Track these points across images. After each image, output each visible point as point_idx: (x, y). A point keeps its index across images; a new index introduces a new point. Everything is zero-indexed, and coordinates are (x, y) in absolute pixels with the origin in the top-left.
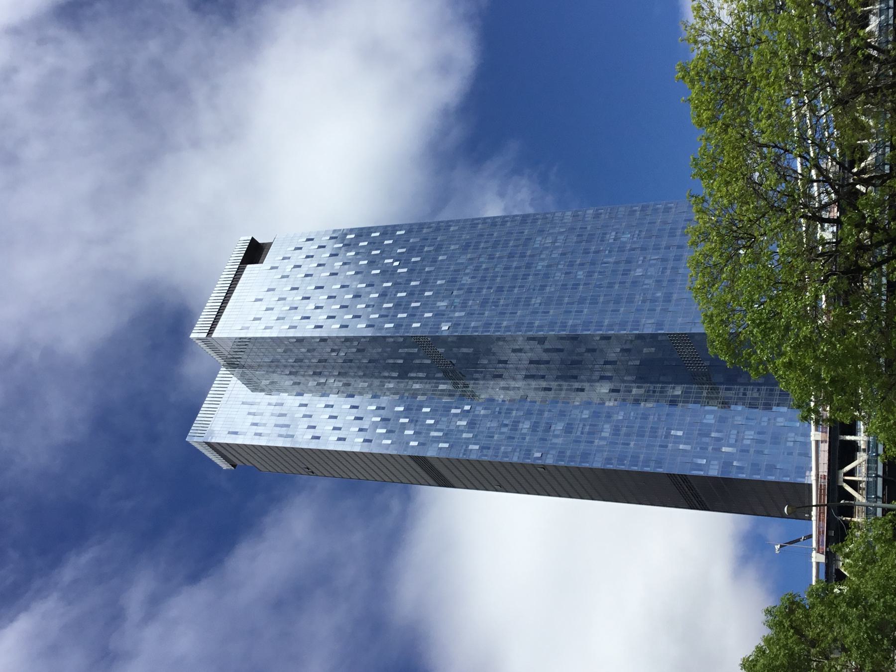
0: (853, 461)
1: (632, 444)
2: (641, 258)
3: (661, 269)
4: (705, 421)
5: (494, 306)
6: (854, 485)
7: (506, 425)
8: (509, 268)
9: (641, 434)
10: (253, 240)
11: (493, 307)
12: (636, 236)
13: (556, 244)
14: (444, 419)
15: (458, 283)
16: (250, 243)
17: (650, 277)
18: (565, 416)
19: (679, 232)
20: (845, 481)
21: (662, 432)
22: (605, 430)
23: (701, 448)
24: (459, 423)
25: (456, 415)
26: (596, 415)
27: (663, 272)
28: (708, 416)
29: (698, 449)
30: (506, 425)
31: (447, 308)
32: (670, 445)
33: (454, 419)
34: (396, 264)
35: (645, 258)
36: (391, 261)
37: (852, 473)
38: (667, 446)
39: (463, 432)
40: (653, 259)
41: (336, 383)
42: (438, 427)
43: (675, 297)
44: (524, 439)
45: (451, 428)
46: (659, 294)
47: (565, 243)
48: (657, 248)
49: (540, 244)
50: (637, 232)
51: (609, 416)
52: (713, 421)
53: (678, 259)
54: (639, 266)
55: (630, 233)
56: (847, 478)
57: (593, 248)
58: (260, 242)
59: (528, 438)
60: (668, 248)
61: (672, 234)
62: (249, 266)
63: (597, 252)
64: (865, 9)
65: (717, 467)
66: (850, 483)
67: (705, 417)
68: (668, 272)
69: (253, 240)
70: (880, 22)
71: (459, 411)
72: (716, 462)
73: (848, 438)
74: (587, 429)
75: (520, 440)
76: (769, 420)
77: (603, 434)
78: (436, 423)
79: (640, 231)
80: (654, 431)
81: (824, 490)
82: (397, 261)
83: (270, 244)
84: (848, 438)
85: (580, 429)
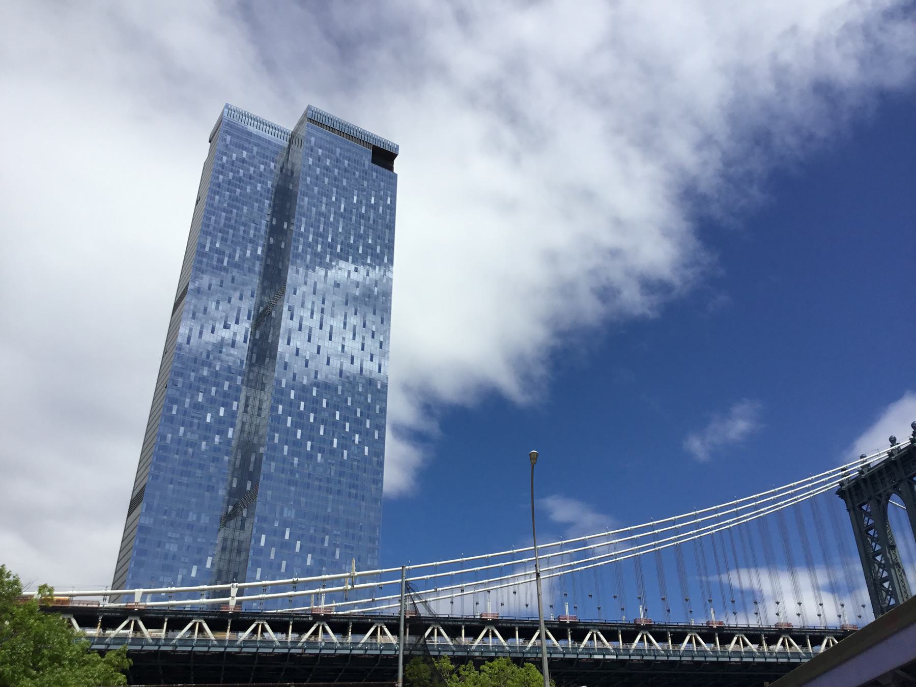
1: (177, 457)
2: (333, 462)
3: (321, 477)
4: (191, 513)
7: (208, 357)
9: (185, 463)
12: (355, 458)
13: (356, 396)
17: (314, 468)
18: (211, 403)
19: (353, 491)
21: (185, 479)
22: (193, 435)
23: (166, 511)
26: (208, 427)
27: (317, 479)
30: (208, 357)
32: (171, 486)
35: (333, 464)
38: (171, 483)
40: (331, 470)
41: (265, 222)
43: (293, 488)
46: (297, 476)
47: (356, 402)
48: (341, 474)
50: (359, 458)
51: (205, 438)
52: (190, 519)
53: (329, 491)
54: (326, 460)
55: (358, 453)
58: (395, 160)
60: (340, 482)
65: (147, 523)
67: (195, 513)
68: (317, 483)
72: (152, 522)
74: (196, 421)
76: (186, 563)
77: (189, 434)
79: (358, 461)
80: (188, 474)
85: (197, 415)
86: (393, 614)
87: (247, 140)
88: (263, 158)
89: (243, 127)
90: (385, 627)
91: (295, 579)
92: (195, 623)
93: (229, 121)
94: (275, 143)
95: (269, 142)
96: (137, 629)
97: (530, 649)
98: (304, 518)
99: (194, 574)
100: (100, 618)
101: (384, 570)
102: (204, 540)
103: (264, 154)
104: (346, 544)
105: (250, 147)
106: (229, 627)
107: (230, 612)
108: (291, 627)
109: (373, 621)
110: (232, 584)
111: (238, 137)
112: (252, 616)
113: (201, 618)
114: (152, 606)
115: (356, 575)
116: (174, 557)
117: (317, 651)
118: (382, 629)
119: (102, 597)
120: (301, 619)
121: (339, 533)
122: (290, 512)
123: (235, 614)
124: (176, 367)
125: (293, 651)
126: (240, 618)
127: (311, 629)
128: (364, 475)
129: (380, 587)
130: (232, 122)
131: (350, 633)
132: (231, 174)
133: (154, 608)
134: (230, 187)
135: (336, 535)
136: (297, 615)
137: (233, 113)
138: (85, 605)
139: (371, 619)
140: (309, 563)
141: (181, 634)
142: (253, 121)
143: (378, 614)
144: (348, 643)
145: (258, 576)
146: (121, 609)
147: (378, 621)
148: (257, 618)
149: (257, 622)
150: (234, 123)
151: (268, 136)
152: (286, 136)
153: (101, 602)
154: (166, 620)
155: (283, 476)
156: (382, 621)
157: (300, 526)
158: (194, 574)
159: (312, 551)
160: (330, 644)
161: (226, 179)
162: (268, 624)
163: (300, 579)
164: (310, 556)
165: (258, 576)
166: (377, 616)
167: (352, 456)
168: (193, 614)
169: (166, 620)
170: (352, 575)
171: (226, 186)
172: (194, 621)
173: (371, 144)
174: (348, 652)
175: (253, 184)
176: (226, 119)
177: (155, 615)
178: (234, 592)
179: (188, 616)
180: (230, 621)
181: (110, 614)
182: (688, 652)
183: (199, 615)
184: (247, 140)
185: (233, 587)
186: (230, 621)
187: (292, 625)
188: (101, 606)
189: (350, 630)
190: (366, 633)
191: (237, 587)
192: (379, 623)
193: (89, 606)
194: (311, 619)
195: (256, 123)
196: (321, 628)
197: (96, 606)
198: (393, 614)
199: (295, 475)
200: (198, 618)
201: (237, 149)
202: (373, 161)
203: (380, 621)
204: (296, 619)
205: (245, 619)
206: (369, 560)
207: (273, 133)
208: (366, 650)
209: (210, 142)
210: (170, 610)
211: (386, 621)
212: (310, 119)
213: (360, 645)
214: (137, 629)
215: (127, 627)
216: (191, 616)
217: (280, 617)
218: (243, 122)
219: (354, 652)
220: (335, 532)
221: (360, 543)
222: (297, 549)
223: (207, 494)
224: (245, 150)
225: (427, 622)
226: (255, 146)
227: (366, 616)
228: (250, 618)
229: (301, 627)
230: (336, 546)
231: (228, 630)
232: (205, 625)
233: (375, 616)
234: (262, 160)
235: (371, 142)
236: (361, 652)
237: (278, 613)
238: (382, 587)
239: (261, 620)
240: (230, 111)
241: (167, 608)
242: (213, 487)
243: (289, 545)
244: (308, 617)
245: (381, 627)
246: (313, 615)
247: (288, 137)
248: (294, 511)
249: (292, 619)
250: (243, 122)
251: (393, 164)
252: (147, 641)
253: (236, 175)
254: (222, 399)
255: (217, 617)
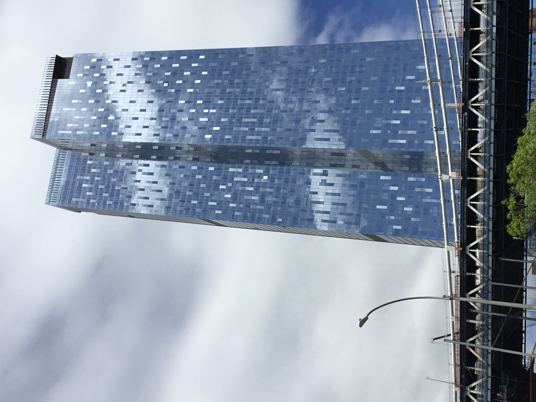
0: (478, 94)
2: (334, 89)
4: (383, 198)
5: (239, 123)
6: (480, 7)
8: (245, 93)
10: (57, 57)
11: (238, 124)
12: (329, 71)
14: (216, 192)
15: (211, 103)
16: (56, 60)
18: (294, 192)
19: (357, 69)
20: (470, 252)
24: (226, 196)
25: (223, 190)
28: (384, 194)
29: (380, 217)
31: (207, 123)
33: (223, 193)
34: (166, 85)
36: (162, 82)
37: (477, 51)
39: (229, 202)
40: (343, 91)
42: (213, 198)
44: (270, 208)
45: (222, 199)
48: (344, 82)
49: (264, 74)
50: (329, 67)
52: (387, 198)
53: (359, 90)
56: (473, 105)
57: (300, 80)
59: (272, 208)
61: (353, 72)
62: (59, 80)
63: (303, 83)
64: (473, 129)
66: (476, 58)
69: (57, 56)
70: (486, 92)
71: (224, 187)
73: (471, 321)
75: (267, 209)
78: (211, 195)
79: (331, 67)
81: (460, 109)
82: (166, 82)
83: (71, 59)
84: (471, 321)
86: (462, 43)
87: (73, 185)
88: (85, 170)
89: (62, 189)
90: (472, 49)
91: (434, 129)
92: (471, 204)
93: (60, 201)
94: (70, 161)
95: (70, 166)
96: (476, 247)
97: (487, 119)
98: (382, 109)
99: (430, 190)
100: (468, 274)
101: (425, 55)
102: (403, 185)
103: (82, 170)
104: (402, 71)
105: (78, 182)
106: (474, 178)
107: (462, 179)
108: (473, 129)
109: (468, 60)
110: (439, 179)
111: (72, 192)
112: (464, 161)
113: (467, 200)
114: (458, 237)
115: (429, 79)
116: (417, 207)
117: (493, 107)
118: (474, 52)
119: (452, 274)
120: (466, 121)
121: (393, 78)
122: (377, 122)
123: (463, 174)
124: (268, 221)
125: (492, 127)
126: (466, 170)
127: (475, 289)
128: (343, 61)
129: (439, 56)
130: (60, 198)
131: (478, 79)
132: (104, 195)
133: (460, 236)
134: (115, 194)
135: (395, 81)
136: (462, 125)
137: (52, 198)
138: (459, 286)
139: (466, 62)
140: (419, 101)
141: (480, 215)
142: (56, 181)
143: (462, 56)
144: (486, 81)
145: (431, 142)
146: (461, 260)
147: (468, 57)
148: (466, 157)
149: (469, 157)
150: (61, 196)
151: (65, 168)
152: (62, 153)
153: (456, 274)
154: (468, 226)
155: (348, 131)
156: (468, 52)
157: (389, 112)
158: (430, 190)
159: (409, 99)
160: (487, 96)
161: (108, 198)
162: (471, 147)
163: (434, 126)
164: (413, 101)
165: (431, 142)
166: (464, 57)
167: (328, 74)
168: (464, 206)
169: (468, 226)
170: (430, 82)
171: (115, 198)
172: (469, 206)
173: (52, 80)
174: (493, 82)
175: (109, 177)
176: (59, 204)
177: (465, 234)
178: (445, 177)
179: (465, 210)
180: (469, 178)
181: (465, 267)
182: (484, 210)
183: (464, 202)
184: (73, 185)
185: (442, 178)
186: (469, 178)
187: (471, 128)
188: (459, 274)
189: (475, 79)
190: (478, 66)
191: (441, 175)
192: (469, 55)
193: (459, 282)
194: (466, 114)
195: (56, 179)
196: (473, 105)
197: (459, 278)
198: (462, 5)
199: (348, 121)
200: (467, 202)
201: (82, 192)
202: (68, 78)
203: (468, 55)
204: (466, 126)
205: (467, 166)
206: (415, 49)
207: (62, 164)
208: (492, 65)
209: (80, 212)
210: (461, 224)
211: (468, 49)
212: (43, 136)
213: (488, 70)
214: (476, 247)
215: (474, 254)
216: (465, 208)
217: (465, 139)
218: (59, 189)
219: (494, 76)
220: (393, 82)
221: (401, 58)
222: (408, 112)
223: (367, 187)
224: (82, 185)
225: (468, 12)
226: (76, 177)
227: (463, 67)
228: (466, 163)
229: (472, 121)
230: (404, 79)
231: (476, 178)
232: (472, 197)
233: (464, 59)
234: (86, 171)
235: (51, 80)
236: (494, 70)
237: (462, 140)
238: (440, 55)
239: (467, 154)
240: (52, 200)
241: (459, 227)
242: (361, 183)
243: (405, 119)
244: (465, 116)
245: (473, 53)
246: (463, 113)
247: (62, 151)
248: (376, 119)
249: (466, 129)
250: (59, 189)
251: (65, 58)
252: (485, 286)
253: (104, 190)
254: (290, 184)
255: (466, 188)
